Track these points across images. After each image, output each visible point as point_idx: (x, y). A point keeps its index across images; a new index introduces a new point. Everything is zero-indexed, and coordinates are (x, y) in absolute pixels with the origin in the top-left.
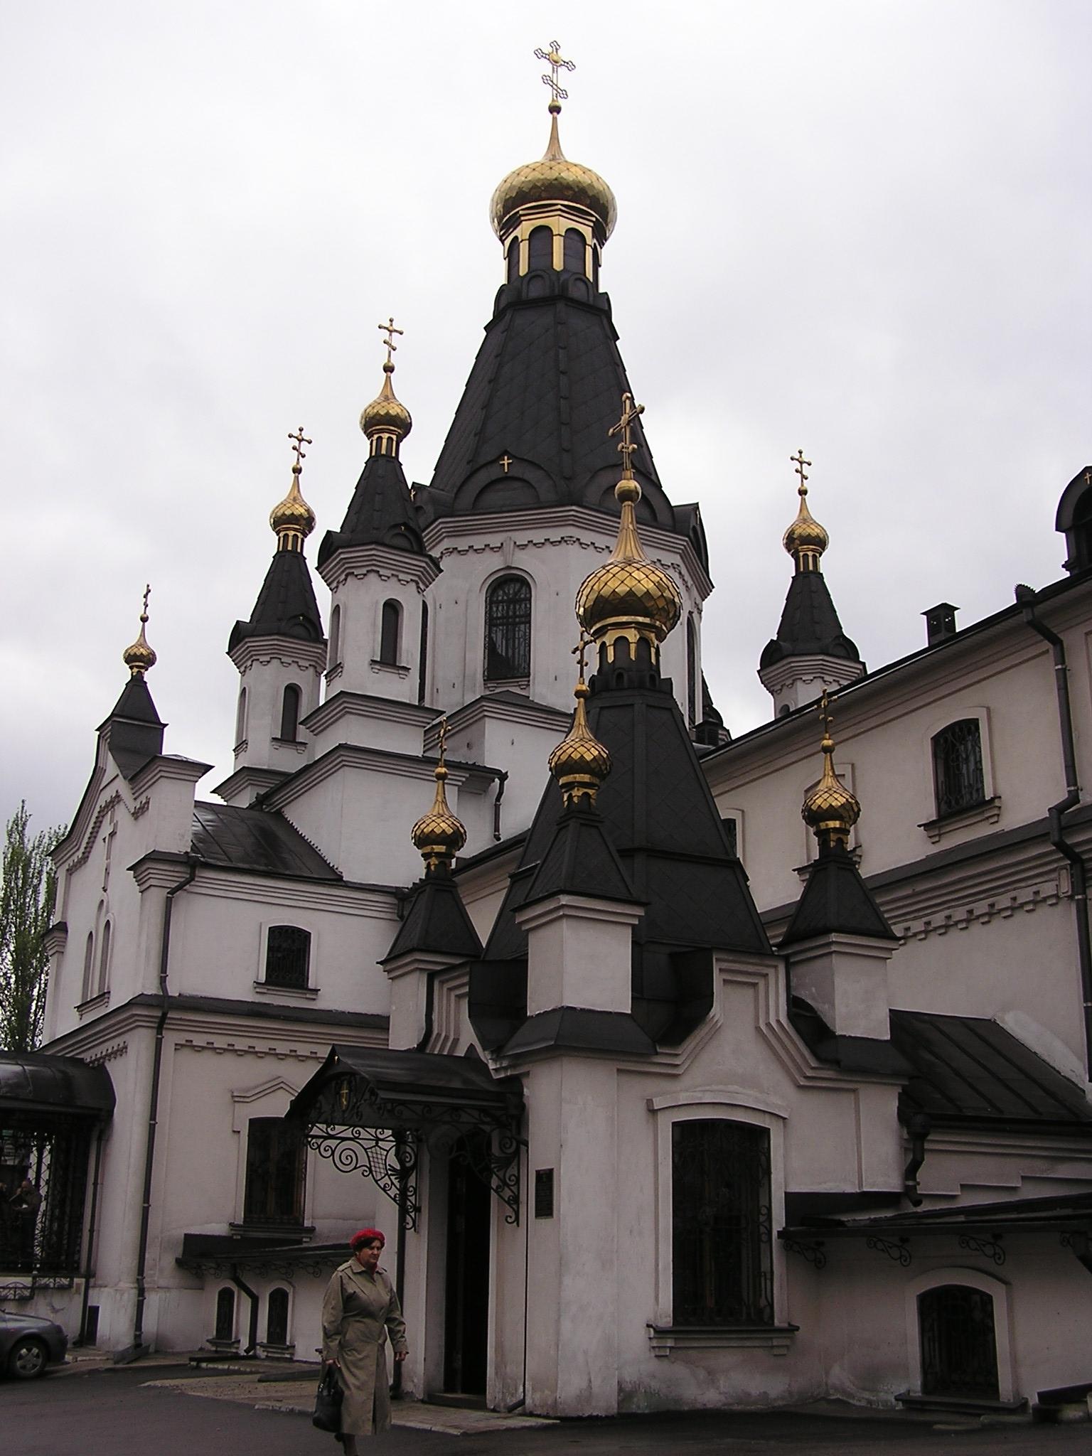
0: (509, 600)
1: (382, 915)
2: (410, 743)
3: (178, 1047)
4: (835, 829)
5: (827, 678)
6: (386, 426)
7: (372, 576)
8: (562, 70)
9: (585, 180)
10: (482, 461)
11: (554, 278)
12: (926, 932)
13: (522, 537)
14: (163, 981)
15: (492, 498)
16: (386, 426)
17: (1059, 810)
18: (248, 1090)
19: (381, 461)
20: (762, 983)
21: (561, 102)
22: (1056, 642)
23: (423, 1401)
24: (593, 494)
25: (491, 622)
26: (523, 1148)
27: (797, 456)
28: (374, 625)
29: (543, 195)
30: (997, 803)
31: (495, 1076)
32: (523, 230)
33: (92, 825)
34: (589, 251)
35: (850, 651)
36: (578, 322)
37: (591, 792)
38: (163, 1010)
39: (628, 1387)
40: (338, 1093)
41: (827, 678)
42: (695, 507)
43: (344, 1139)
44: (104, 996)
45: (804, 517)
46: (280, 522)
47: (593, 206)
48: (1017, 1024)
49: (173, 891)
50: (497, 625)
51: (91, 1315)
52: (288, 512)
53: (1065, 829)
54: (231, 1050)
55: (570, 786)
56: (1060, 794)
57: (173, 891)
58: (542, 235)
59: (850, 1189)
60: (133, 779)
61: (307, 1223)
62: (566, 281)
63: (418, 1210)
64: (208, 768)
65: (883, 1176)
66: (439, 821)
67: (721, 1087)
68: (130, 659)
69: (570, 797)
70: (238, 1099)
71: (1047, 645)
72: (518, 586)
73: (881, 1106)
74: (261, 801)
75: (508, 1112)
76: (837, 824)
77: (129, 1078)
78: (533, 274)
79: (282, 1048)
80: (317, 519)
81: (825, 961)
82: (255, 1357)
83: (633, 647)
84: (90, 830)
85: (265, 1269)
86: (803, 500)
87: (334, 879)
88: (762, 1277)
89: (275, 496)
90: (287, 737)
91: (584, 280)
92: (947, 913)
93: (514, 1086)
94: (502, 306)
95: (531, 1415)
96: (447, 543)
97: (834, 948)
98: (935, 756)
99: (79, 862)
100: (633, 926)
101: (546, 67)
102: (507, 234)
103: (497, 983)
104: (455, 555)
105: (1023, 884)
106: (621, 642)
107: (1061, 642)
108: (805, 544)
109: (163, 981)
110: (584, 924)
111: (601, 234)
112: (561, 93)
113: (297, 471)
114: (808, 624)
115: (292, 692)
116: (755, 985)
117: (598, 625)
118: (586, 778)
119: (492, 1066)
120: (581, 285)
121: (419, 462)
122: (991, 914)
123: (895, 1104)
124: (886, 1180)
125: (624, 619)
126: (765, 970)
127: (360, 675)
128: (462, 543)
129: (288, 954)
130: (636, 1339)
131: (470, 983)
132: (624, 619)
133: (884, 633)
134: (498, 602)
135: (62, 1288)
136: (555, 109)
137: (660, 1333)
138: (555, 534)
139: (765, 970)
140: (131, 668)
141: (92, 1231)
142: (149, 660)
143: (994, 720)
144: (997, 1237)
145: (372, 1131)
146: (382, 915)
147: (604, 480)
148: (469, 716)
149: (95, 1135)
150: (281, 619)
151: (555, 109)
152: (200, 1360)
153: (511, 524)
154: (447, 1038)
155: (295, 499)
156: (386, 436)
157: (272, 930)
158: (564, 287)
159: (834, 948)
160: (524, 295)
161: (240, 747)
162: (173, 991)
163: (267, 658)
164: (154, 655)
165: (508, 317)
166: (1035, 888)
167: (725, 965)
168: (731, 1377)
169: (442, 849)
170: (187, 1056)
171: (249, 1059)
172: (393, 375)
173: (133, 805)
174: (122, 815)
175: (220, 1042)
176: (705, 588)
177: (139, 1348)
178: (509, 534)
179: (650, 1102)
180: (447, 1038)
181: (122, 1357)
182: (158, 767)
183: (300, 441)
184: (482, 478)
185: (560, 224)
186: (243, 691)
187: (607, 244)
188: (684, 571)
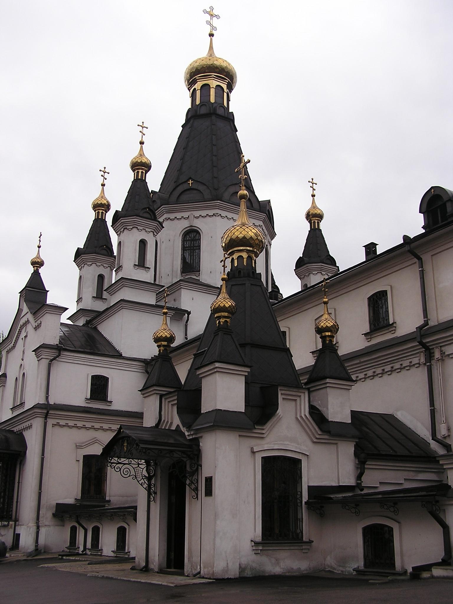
0: (192, 240)
1: (138, 370)
2: (150, 299)
3: (54, 425)
4: (328, 336)
5: (323, 273)
6: (141, 167)
7: (135, 229)
8: (215, 19)
9: (224, 65)
10: (180, 182)
11: (211, 106)
12: (365, 378)
13: (197, 214)
14: (47, 398)
15: (184, 197)
16: (141, 167)
17: (420, 328)
18: (83, 443)
19: (139, 181)
20: (298, 399)
21: (214, 32)
22: (419, 259)
23: (158, 572)
24: (226, 195)
25: (184, 249)
26: (200, 467)
27: (311, 181)
28: (136, 250)
29: (207, 71)
30: (394, 325)
31: (188, 438)
32: (198, 86)
33: (17, 332)
34: (225, 94)
35: (332, 261)
36: (221, 124)
37: (228, 320)
38: (47, 410)
39: (243, 566)
40: (123, 445)
41: (323, 273)
42: (269, 201)
43: (125, 464)
44: (22, 404)
45: (314, 206)
46: (96, 207)
47: (228, 76)
48: (403, 416)
49: (52, 360)
50: (186, 250)
51: (17, 537)
52: (99, 202)
53: (423, 336)
54: (75, 426)
55: (219, 318)
56: (421, 322)
57: (52, 360)
58: (206, 88)
59: (334, 484)
60: (34, 314)
61: (107, 499)
62: (216, 107)
63: (155, 493)
64: (67, 309)
65: (348, 478)
66: (164, 332)
67: (281, 442)
68: (33, 263)
69: (219, 322)
70: (78, 447)
71: (416, 260)
72: (195, 234)
73: (347, 451)
74: (88, 323)
75: (193, 453)
76: (329, 334)
77: (32, 439)
78: (202, 104)
79: (97, 426)
80: (111, 205)
81: (324, 390)
82: (86, 554)
83: (245, 260)
84: (16, 335)
85: (90, 517)
86: (313, 199)
87: (118, 355)
88: (298, 521)
89: (94, 196)
90: (99, 296)
91: (223, 107)
92: (374, 370)
93: (196, 442)
94: (189, 117)
95: (203, 578)
96: (166, 216)
97: (328, 385)
98: (369, 305)
99: (12, 348)
100: (245, 376)
101: (208, 17)
102: (191, 87)
103: (189, 399)
104: (169, 221)
105: (405, 359)
106: (240, 258)
107: (421, 259)
108: (314, 217)
109: (47, 398)
110: (226, 375)
111: (230, 87)
112: (214, 28)
113: (103, 185)
114: (315, 251)
115: (101, 278)
116: (295, 400)
117: (230, 251)
118: (226, 314)
119: (186, 434)
120: (221, 108)
121: (154, 181)
122: (392, 371)
123: (353, 449)
124: (349, 480)
125: (242, 248)
126: (300, 394)
127: (129, 271)
128: (172, 216)
129: (99, 387)
130: (247, 546)
131: (177, 399)
132: (242, 248)
133: (347, 254)
134: (187, 241)
135: (4, 526)
136: (211, 35)
137: (257, 544)
138: (211, 212)
139: (300, 394)
140: (34, 267)
141: (17, 502)
142: (41, 264)
143: (394, 291)
144: (395, 504)
145: (136, 460)
146: (138, 370)
147: (232, 190)
148: (175, 287)
149: (18, 463)
150: (96, 247)
151: (211, 35)
152: (63, 556)
153: (194, 208)
154: (168, 422)
155: (102, 197)
156: (140, 171)
157: (93, 377)
158: (215, 109)
159: (328, 385)
160: (198, 112)
161: (79, 300)
162: (51, 402)
163: (91, 263)
164: (43, 262)
165: (191, 121)
166: (410, 360)
167: (283, 392)
168: (285, 561)
169: (166, 343)
170: (57, 429)
171: (83, 430)
172: (143, 146)
173: (35, 324)
174: (30, 328)
175: (71, 423)
176: (273, 235)
177: (37, 550)
178: (192, 212)
179: (252, 448)
180: (168, 422)
181: (30, 554)
182: (45, 309)
183: (104, 173)
184: (180, 189)
185: (214, 83)
186: (80, 277)
187: (233, 92)
188: (264, 228)
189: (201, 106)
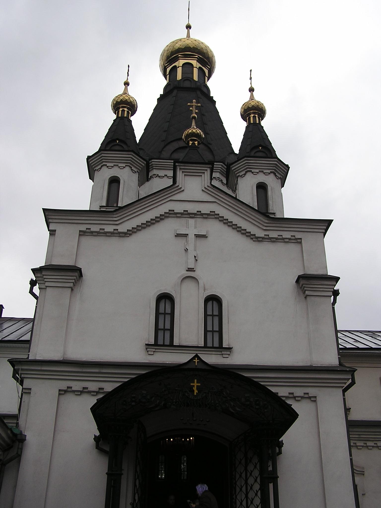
78: (184, 79)
94: (168, 90)
189: (184, 80)
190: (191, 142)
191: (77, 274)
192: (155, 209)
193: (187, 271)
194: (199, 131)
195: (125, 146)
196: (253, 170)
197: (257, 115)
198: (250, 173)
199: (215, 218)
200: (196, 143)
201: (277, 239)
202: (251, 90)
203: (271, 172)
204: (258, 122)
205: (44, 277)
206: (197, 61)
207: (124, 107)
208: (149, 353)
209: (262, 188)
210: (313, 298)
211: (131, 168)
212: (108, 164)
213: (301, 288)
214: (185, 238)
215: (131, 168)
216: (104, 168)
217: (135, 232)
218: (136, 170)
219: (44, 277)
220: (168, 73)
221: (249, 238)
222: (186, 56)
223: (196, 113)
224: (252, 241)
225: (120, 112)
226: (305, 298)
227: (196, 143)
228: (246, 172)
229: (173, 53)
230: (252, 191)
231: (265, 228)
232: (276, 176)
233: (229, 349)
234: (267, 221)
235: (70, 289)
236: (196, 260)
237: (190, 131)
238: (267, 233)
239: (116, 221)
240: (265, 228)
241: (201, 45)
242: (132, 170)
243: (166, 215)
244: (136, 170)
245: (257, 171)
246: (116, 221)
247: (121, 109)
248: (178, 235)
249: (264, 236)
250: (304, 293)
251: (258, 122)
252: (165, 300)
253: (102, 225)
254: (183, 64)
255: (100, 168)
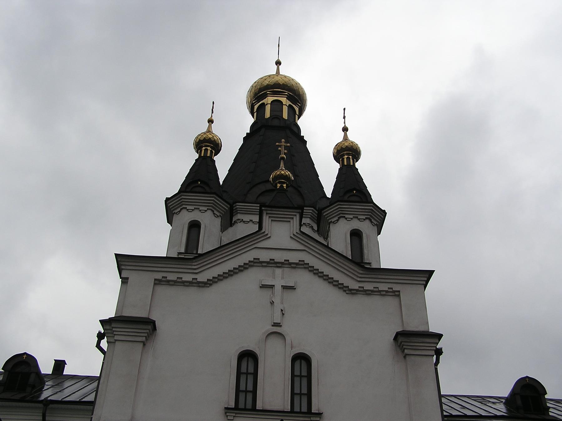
32: (270, 99)
58: (277, 104)
78: (272, 117)
189: (273, 119)
190: (279, 185)
191: (150, 327)
192: (239, 257)
193: (273, 326)
194: (288, 173)
195: (207, 189)
196: (347, 216)
197: (351, 157)
198: (344, 219)
199: (305, 268)
200: (285, 185)
201: (372, 291)
202: (345, 129)
203: (366, 218)
204: (352, 164)
205: (114, 329)
206: (287, 98)
207: (208, 146)
208: (229, 418)
209: (356, 235)
210: (413, 358)
211: (213, 211)
212: (188, 207)
213: (399, 346)
214: (271, 289)
215: (213, 211)
216: (184, 211)
217: (216, 282)
218: (218, 214)
219: (114, 329)
220: (255, 111)
221: (341, 291)
222: (275, 93)
223: (285, 154)
224: (345, 294)
225: (203, 151)
226: (405, 357)
227: (285, 185)
228: (339, 218)
229: (261, 90)
230: (346, 238)
231: (359, 279)
232: (372, 222)
233: (319, 414)
234: (361, 272)
235: (142, 344)
236: (283, 314)
237: (278, 173)
238: (361, 285)
239: (195, 269)
240: (359, 279)
241: (292, 81)
242: (214, 214)
243: (250, 264)
244: (218, 214)
245: (351, 216)
246: (195, 269)
247: (204, 148)
248: (263, 287)
249: (358, 288)
250: (403, 352)
251: (352, 164)
252: (248, 358)
253: (180, 274)
254: (272, 102)
255: (180, 211)
